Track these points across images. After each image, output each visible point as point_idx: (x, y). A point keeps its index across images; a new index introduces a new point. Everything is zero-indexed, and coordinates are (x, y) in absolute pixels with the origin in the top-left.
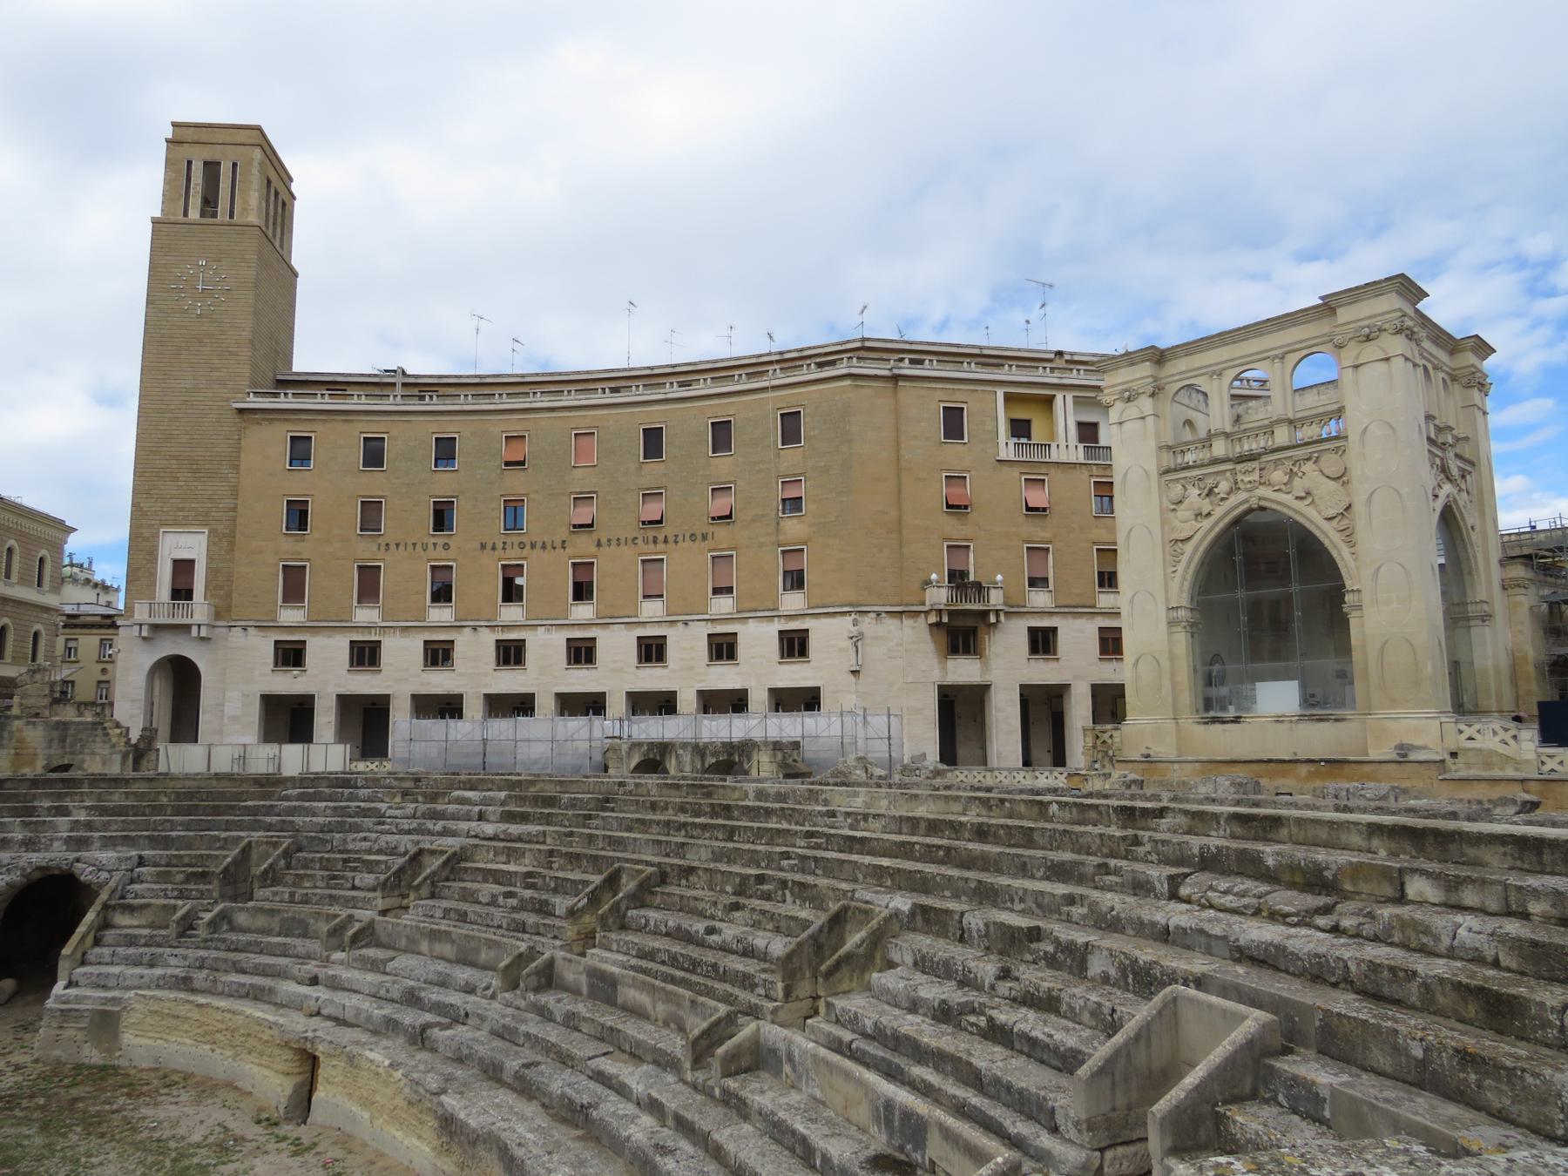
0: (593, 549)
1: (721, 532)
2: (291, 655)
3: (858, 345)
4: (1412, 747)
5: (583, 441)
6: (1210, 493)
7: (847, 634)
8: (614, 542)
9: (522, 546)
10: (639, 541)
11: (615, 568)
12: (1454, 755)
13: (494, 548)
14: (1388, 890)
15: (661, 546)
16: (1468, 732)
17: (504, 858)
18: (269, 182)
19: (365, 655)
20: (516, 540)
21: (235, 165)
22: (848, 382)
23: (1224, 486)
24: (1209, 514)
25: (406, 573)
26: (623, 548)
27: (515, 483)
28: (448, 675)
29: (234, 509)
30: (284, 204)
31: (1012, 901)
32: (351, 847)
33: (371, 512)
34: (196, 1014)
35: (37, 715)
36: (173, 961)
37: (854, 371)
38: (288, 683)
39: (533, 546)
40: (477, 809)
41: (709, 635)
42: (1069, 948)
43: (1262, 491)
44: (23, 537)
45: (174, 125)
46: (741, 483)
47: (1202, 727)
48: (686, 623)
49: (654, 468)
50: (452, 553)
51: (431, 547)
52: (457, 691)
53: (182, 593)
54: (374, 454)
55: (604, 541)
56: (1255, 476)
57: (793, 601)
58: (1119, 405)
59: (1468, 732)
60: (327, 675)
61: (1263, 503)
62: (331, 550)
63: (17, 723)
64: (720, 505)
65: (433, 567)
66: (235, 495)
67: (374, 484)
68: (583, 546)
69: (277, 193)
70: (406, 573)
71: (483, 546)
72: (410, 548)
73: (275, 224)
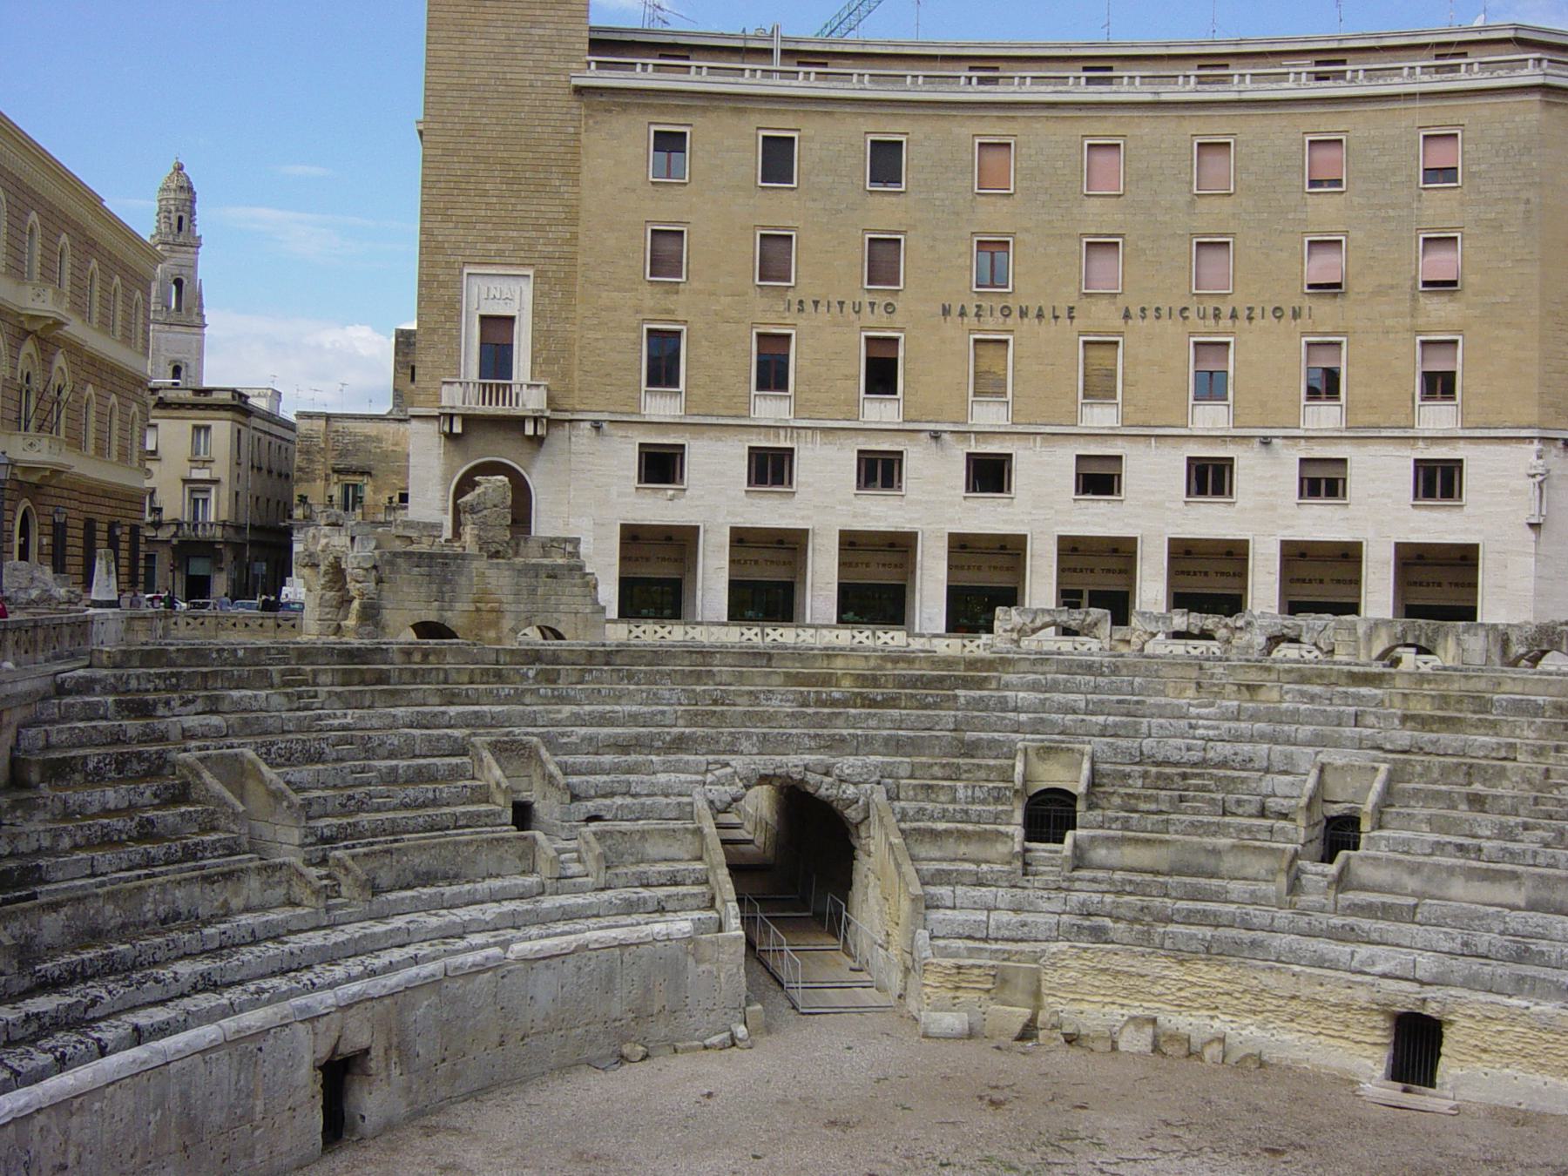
0: (1118, 323)
1: (1325, 312)
2: (661, 466)
3: (1510, 34)
5: (1101, 158)
7: (1523, 470)
8: (1151, 313)
9: (1006, 312)
10: (1192, 314)
13: (962, 314)
15: (1225, 323)
22: (1537, 97)
25: (828, 351)
26: (1165, 322)
32: (1176, 757)
33: (774, 255)
34: (1176, 972)
35: (497, 554)
36: (1046, 906)
37: (1551, 81)
38: (658, 508)
40: (1353, 709)
41: (1302, 461)
44: (126, 271)
46: (1352, 234)
48: (1266, 442)
50: (898, 320)
52: (907, 528)
54: (778, 159)
55: (1135, 311)
57: (1437, 417)
60: (715, 499)
62: (719, 312)
63: (475, 564)
64: (1323, 267)
65: (868, 339)
66: (573, 220)
67: (780, 208)
70: (828, 351)
71: (946, 311)
72: (835, 308)
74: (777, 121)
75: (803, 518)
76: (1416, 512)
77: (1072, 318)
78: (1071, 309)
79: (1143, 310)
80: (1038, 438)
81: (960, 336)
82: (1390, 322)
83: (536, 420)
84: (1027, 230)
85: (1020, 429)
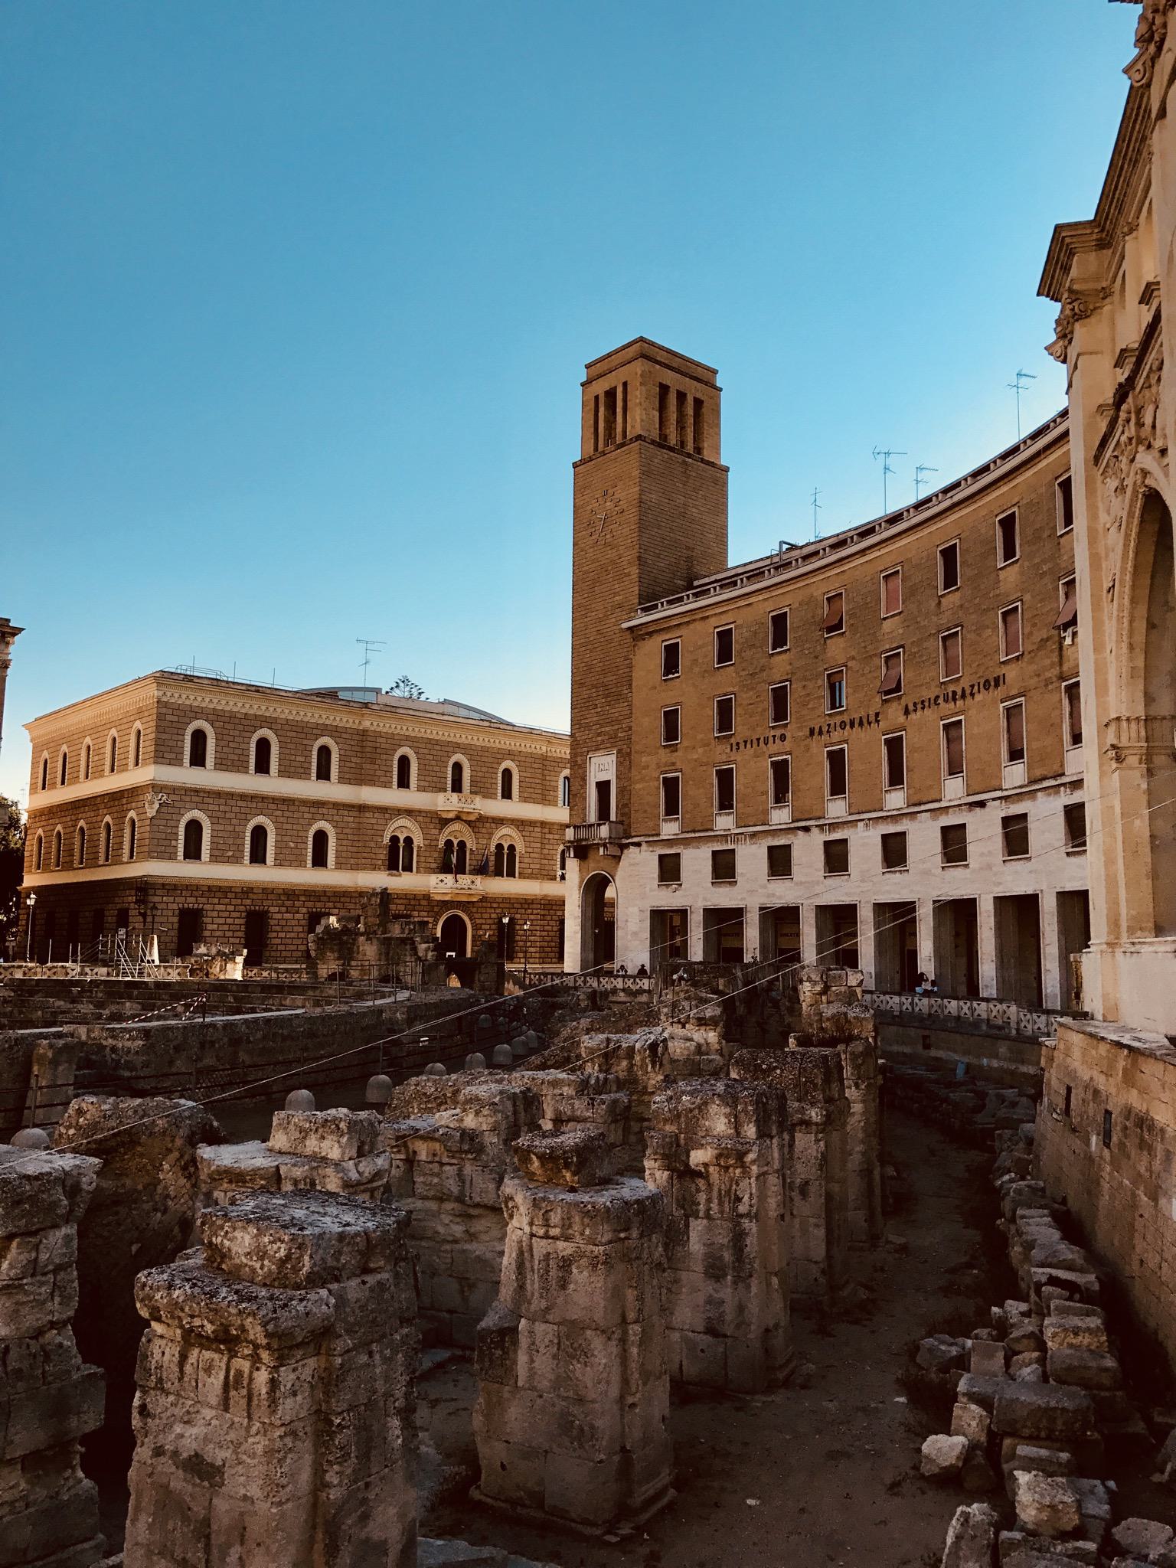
0: (902, 719)
2: (670, 871)
8: (919, 706)
10: (940, 701)
11: (924, 735)
15: (960, 703)
18: (664, 389)
19: (724, 868)
20: (838, 719)
21: (625, 384)
25: (753, 773)
27: (837, 649)
28: (788, 883)
29: (630, 728)
30: (698, 403)
38: (668, 899)
39: (852, 725)
45: (588, 367)
46: (1027, 597)
49: (953, 599)
50: (787, 745)
51: (771, 739)
53: (603, 813)
55: (911, 707)
60: (697, 891)
63: (362, 939)
67: (727, 681)
68: (894, 714)
69: (681, 396)
70: (753, 773)
73: (681, 426)
74: (725, 619)
75: (743, 899)
76: (1072, 859)
77: (878, 721)
78: (877, 715)
79: (915, 704)
80: (861, 824)
81: (820, 753)
82: (1048, 675)
83: (605, 845)
84: (853, 658)
85: (851, 818)
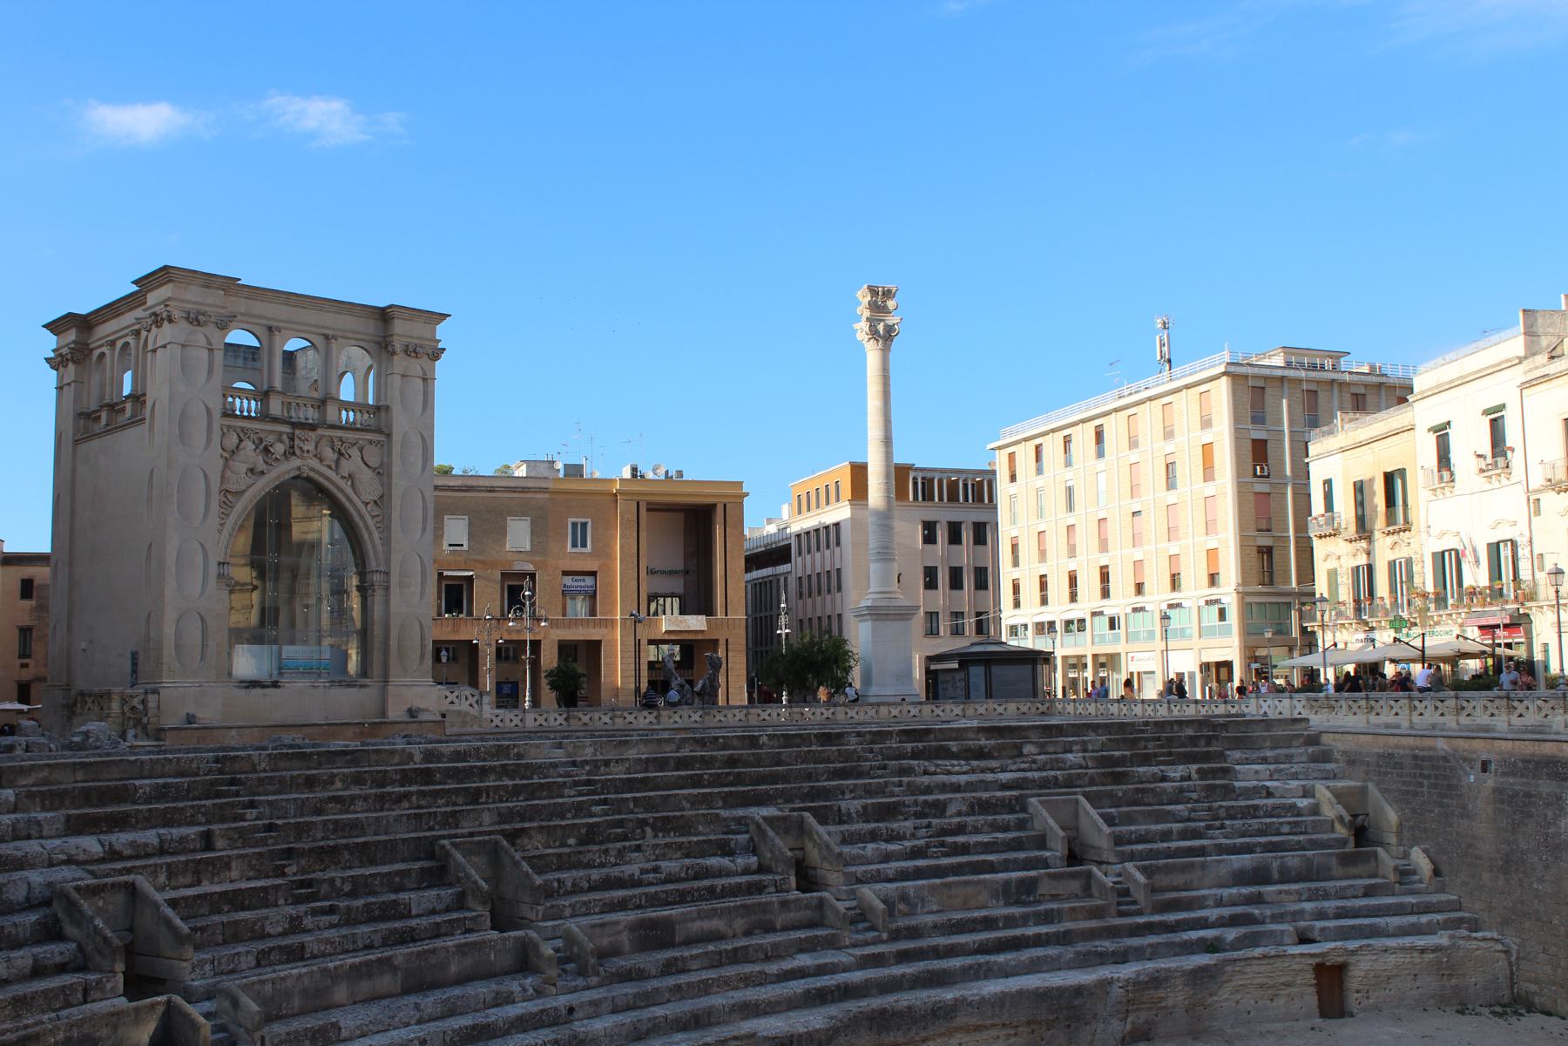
4: (419, 710)
6: (266, 450)
12: (444, 716)
14: (1015, 752)
16: (452, 697)
17: (189, 879)
23: (279, 449)
24: (263, 473)
31: (843, 793)
42: (936, 804)
43: (314, 463)
47: (243, 692)
56: (310, 446)
58: (184, 324)
59: (452, 697)
61: (316, 477)
